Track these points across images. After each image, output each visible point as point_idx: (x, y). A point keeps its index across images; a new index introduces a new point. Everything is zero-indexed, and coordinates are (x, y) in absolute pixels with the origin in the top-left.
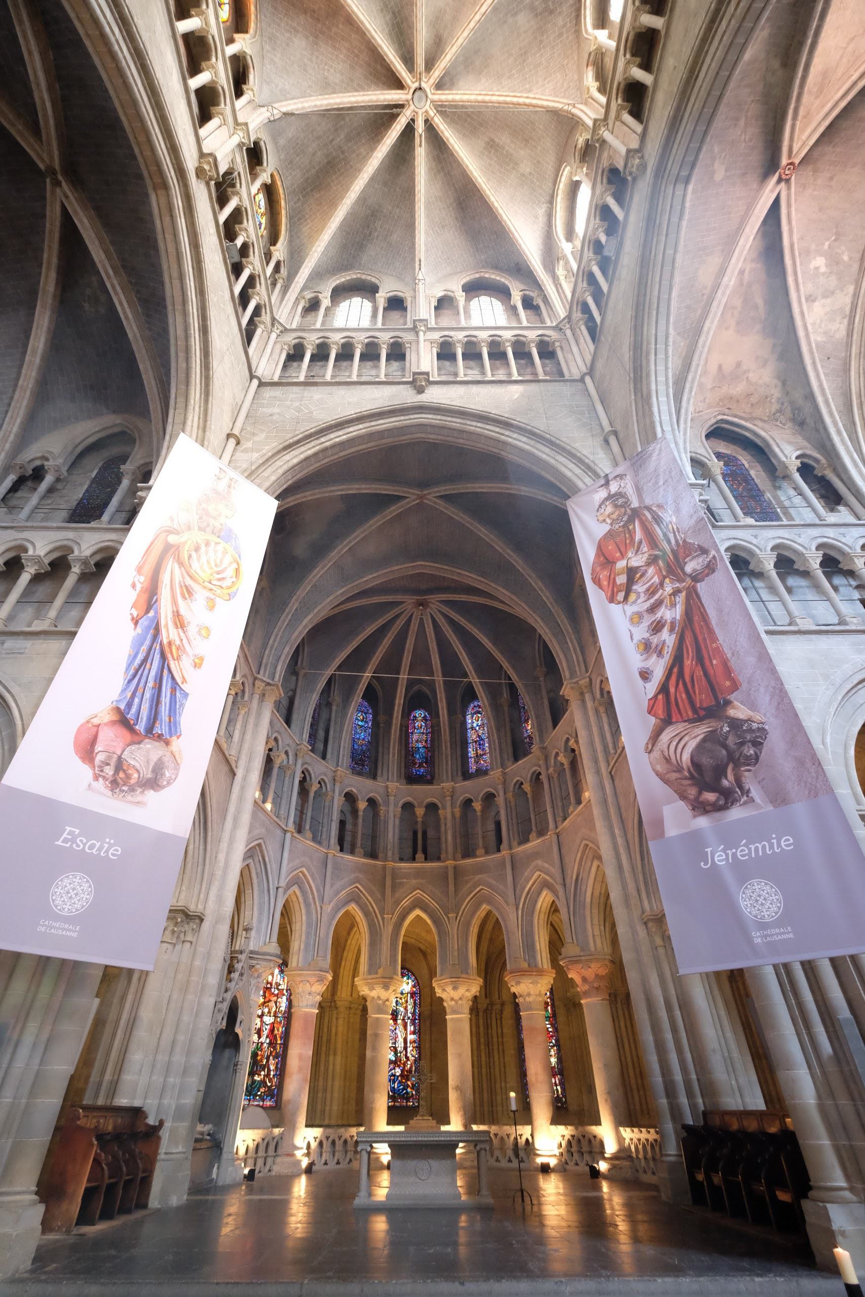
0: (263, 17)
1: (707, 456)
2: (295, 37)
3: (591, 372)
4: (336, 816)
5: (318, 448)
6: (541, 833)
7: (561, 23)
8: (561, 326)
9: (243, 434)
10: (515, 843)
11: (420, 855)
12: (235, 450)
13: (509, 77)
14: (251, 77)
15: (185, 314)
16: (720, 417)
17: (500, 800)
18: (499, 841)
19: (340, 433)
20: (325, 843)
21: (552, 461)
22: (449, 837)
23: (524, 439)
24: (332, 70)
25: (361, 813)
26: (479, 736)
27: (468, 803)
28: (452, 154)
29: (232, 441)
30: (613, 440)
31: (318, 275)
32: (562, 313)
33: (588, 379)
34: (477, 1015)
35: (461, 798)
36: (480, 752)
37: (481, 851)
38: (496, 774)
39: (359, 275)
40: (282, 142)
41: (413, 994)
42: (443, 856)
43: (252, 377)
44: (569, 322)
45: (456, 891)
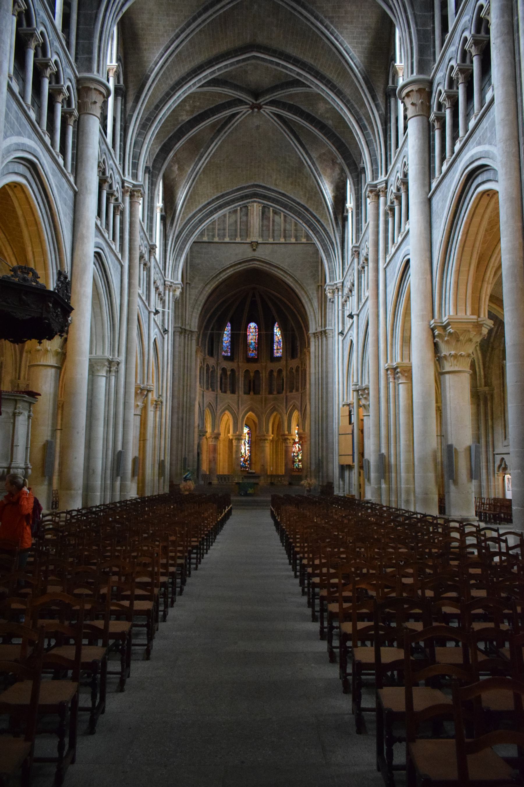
4: (219, 379)
5: (217, 283)
6: (297, 390)
10: (288, 391)
11: (252, 393)
17: (284, 373)
18: (283, 389)
19: (224, 273)
20: (216, 390)
22: (264, 386)
25: (228, 376)
26: (279, 340)
27: (272, 371)
29: (188, 285)
30: (320, 287)
34: (273, 444)
35: (269, 369)
36: (279, 347)
37: (275, 393)
38: (283, 362)
41: (248, 434)
42: (261, 393)
45: (265, 407)
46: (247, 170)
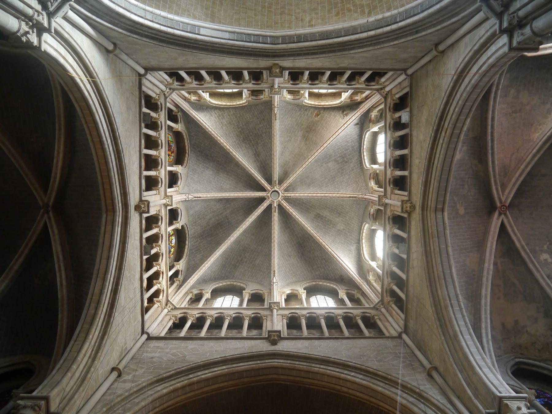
0: (190, 162)
1: (519, 386)
2: (207, 170)
3: (406, 330)
7: (352, 165)
8: (377, 306)
9: (125, 370)
12: (115, 381)
13: (326, 187)
14: (179, 182)
15: (104, 279)
16: (517, 360)
21: (387, 392)
23: (361, 376)
24: (225, 184)
28: (295, 220)
29: (115, 374)
30: (434, 374)
31: (204, 281)
32: (375, 299)
33: (404, 336)
39: (232, 283)
40: (191, 212)
43: (143, 332)
44: (382, 304)
46: (264, 16)
